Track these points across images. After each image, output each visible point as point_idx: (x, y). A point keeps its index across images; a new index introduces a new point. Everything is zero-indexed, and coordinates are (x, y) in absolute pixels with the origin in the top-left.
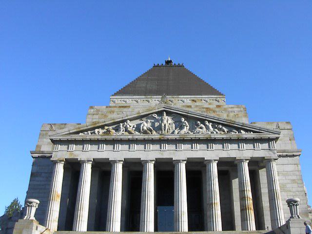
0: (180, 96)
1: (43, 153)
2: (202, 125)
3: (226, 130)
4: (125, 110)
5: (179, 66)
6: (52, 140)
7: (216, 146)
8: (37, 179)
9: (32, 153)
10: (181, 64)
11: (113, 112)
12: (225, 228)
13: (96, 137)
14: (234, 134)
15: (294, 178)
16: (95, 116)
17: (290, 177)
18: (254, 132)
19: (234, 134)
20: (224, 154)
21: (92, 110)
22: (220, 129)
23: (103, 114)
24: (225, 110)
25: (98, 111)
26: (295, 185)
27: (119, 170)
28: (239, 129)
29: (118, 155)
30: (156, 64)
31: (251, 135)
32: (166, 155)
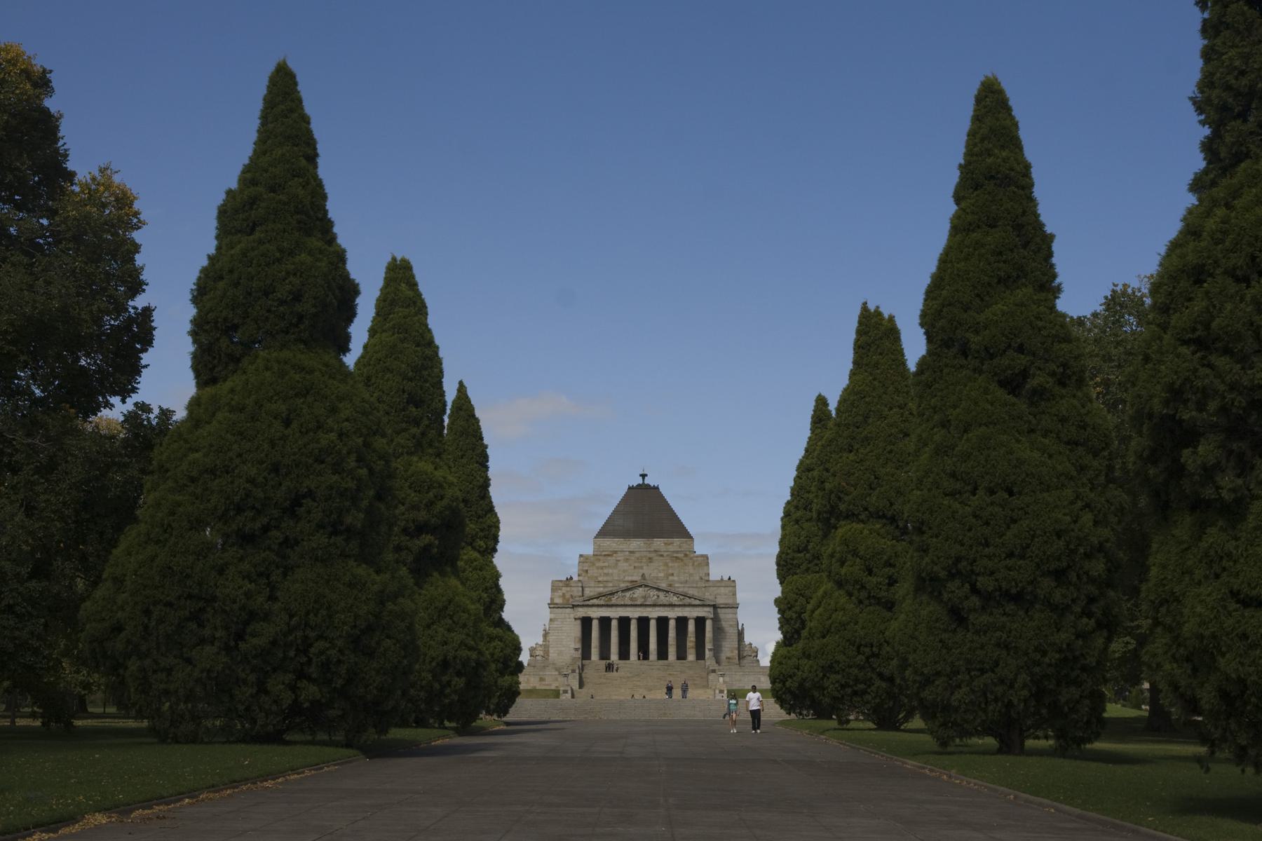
0: (655, 539)
1: (557, 604)
2: (667, 595)
3: (682, 597)
4: (609, 558)
5: (656, 488)
6: (573, 605)
7: (676, 609)
8: (556, 623)
9: (549, 604)
10: (656, 485)
11: (599, 560)
12: (678, 658)
14: (687, 601)
15: (731, 623)
16: (587, 564)
17: (728, 623)
18: (700, 600)
19: (687, 601)
20: (680, 614)
21: (582, 559)
22: (678, 597)
23: (591, 562)
24: (691, 559)
25: (587, 559)
26: (732, 629)
27: (614, 624)
28: (690, 597)
29: (614, 613)
30: (631, 485)
31: (697, 602)
32: (645, 615)
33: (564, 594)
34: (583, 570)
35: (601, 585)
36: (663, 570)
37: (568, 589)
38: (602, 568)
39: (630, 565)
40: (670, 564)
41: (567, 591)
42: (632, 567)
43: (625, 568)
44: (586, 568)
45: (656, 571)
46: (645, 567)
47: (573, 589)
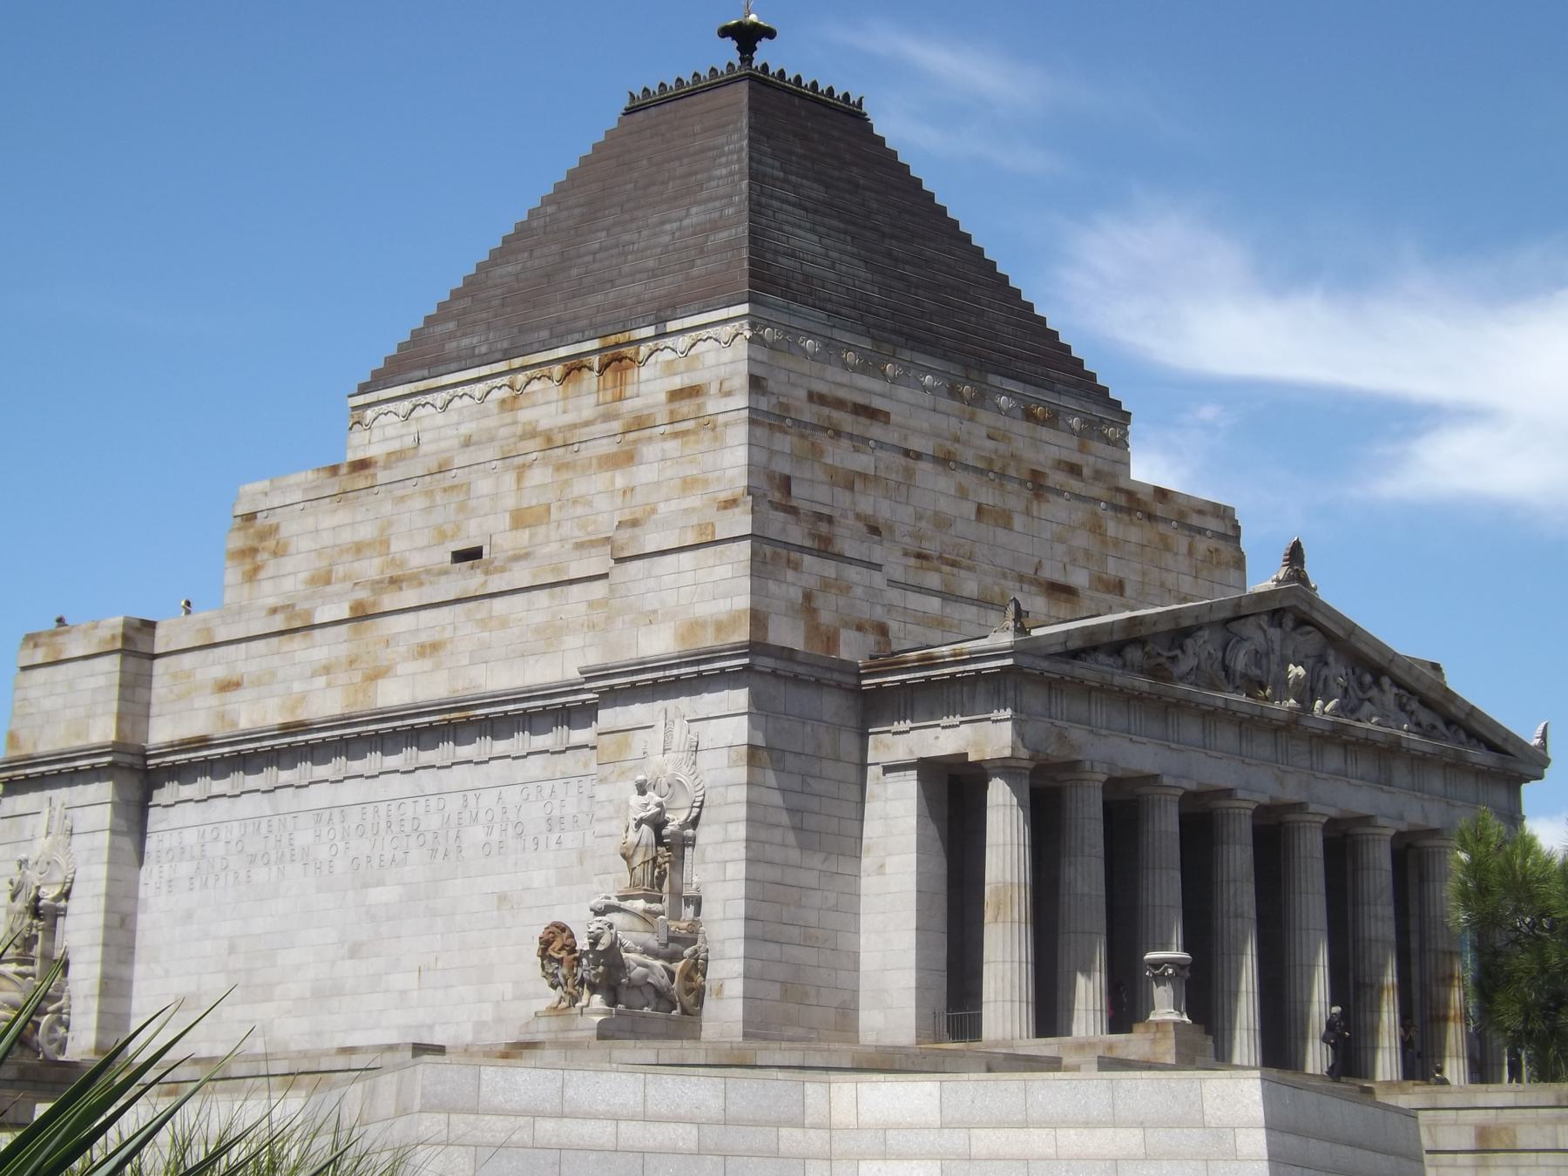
1: (787, 654)
11: (838, 434)
13: (1137, 683)
33: (808, 596)
34: (771, 476)
35: (933, 580)
36: (1087, 552)
37: (829, 569)
38: (849, 481)
39: (963, 493)
40: (1112, 528)
41: (826, 585)
42: (969, 509)
43: (945, 506)
44: (787, 471)
45: (1060, 549)
46: (1018, 522)
47: (853, 573)
